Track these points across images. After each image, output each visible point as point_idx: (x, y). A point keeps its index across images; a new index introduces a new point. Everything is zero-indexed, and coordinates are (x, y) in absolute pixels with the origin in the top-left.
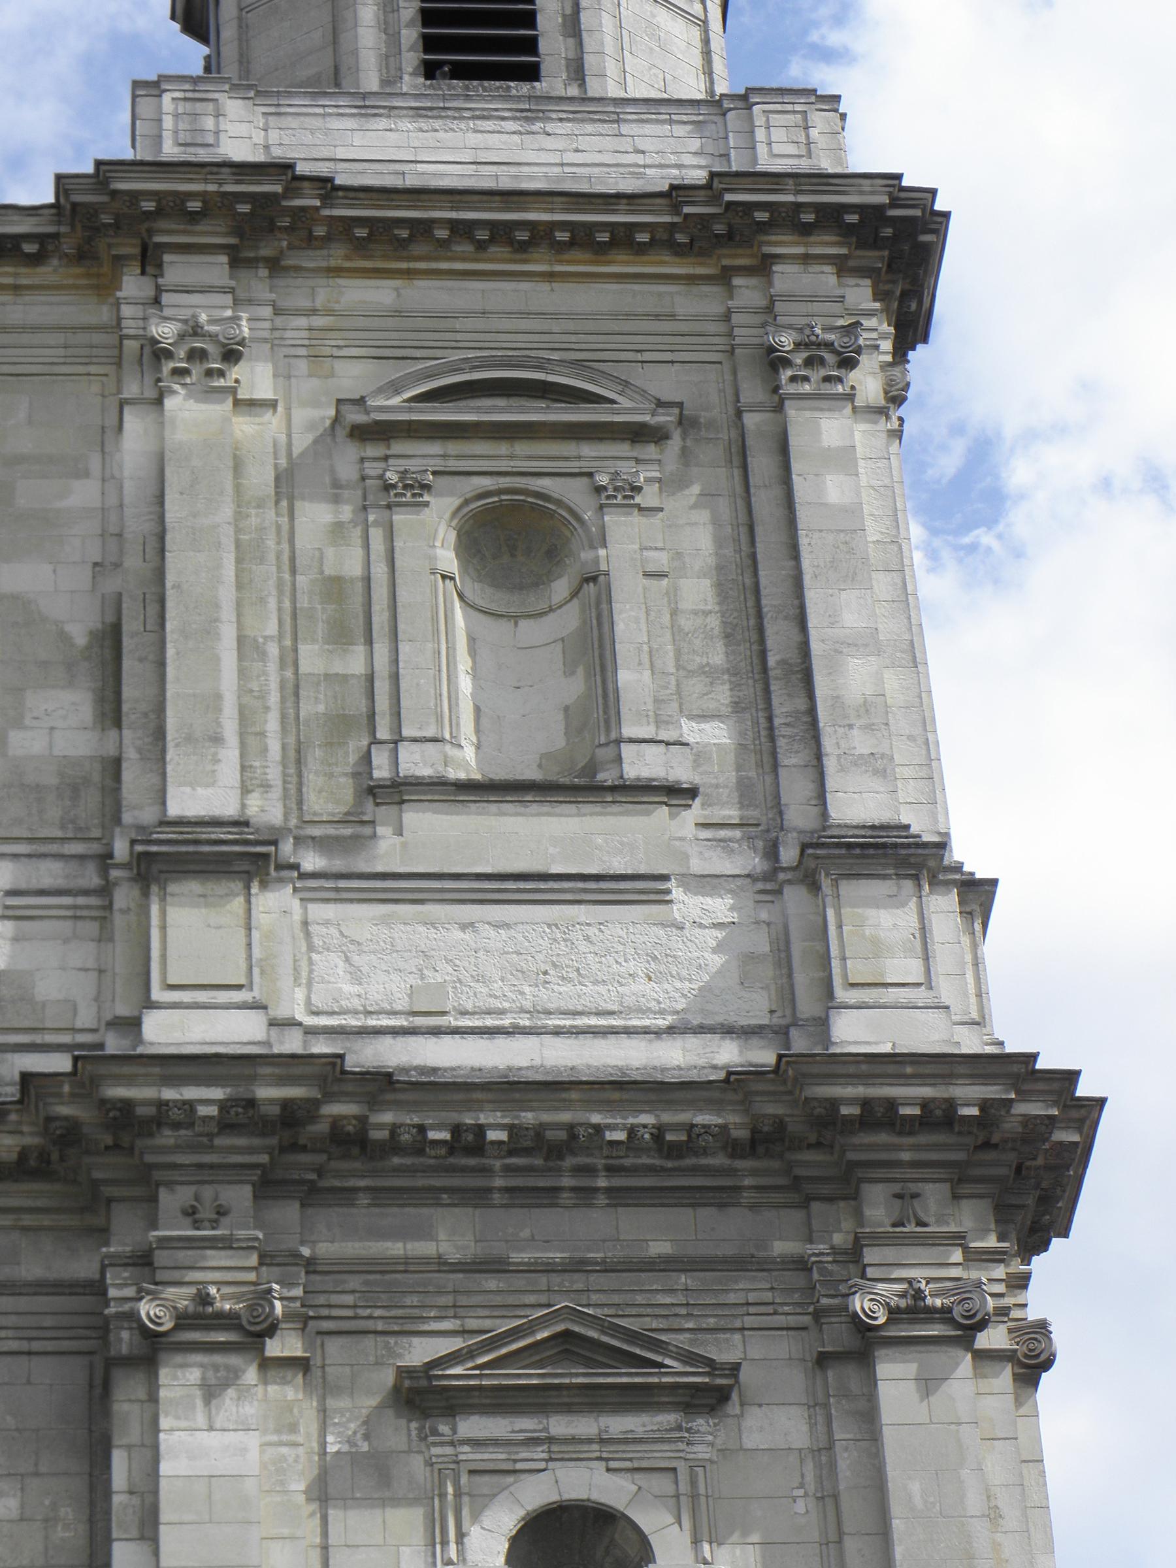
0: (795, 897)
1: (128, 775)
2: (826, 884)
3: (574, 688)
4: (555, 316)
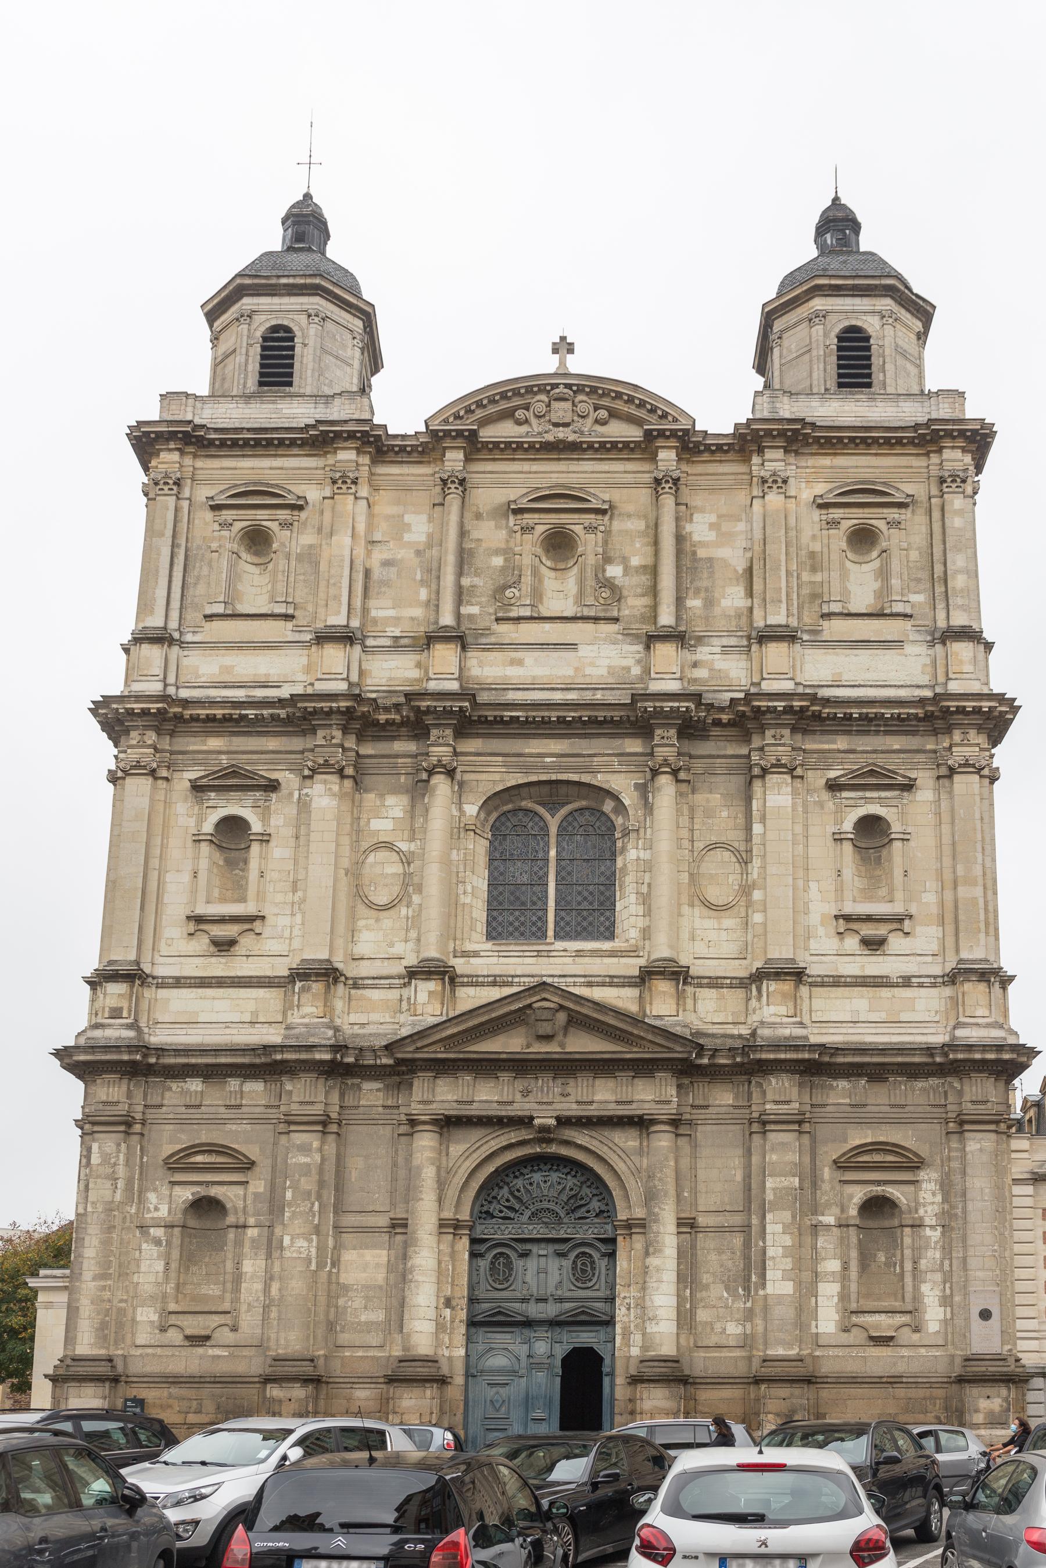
0: (939, 647)
1: (755, 612)
2: (948, 643)
3: (877, 585)
4: (877, 467)
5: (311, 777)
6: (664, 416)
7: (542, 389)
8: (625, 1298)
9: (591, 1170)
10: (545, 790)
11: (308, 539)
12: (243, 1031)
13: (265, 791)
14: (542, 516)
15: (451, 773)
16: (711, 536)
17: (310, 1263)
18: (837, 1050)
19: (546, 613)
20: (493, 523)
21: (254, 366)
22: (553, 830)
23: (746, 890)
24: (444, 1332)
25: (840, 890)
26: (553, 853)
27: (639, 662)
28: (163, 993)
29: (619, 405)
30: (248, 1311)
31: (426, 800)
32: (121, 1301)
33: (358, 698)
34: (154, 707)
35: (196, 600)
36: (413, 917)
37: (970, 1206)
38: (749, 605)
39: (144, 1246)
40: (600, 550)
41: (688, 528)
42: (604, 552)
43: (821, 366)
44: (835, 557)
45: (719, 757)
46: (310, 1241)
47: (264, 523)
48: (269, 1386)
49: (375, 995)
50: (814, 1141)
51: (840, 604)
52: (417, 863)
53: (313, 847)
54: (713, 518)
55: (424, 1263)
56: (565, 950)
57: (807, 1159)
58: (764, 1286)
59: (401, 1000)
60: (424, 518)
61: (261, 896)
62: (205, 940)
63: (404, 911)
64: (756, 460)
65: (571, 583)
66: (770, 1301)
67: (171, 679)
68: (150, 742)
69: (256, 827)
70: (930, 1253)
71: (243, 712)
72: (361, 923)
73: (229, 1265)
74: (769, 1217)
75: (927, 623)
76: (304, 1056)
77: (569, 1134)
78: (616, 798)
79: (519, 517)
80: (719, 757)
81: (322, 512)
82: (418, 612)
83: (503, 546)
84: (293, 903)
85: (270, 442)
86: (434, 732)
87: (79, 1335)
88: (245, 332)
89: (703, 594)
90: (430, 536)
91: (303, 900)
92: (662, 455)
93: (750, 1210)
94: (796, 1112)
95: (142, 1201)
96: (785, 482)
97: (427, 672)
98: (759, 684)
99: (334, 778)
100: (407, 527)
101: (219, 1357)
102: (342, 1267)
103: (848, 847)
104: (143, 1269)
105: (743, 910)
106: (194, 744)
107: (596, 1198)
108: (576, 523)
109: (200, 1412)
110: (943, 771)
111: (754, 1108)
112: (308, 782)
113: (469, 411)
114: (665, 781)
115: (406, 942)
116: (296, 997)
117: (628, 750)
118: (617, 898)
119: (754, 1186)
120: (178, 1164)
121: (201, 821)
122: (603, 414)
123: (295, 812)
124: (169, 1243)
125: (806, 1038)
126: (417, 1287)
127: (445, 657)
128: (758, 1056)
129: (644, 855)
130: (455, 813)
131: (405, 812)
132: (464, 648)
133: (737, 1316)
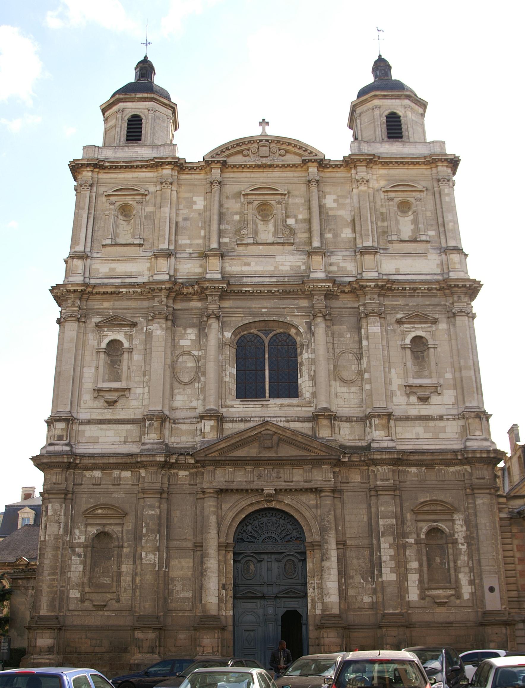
0: (443, 256)
3: (412, 227)
5: (152, 320)
6: (311, 153)
7: (255, 141)
8: (312, 583)
9: (292, 516)
10: (263, 324)
11: (150, 209)
12: (120, 446)
13: (130, 327)
14: (257, 197)
15: (218, 318)
16: (335, 205)
17: (156, 566)
18: (411, 453)
19: (260, 242)
20: (234, 200)
21: (124, 132)
22: (267, 344)
23: (360, 373)
24: (222, 602)
25: (406, 373)
26: (267, 356)
27: (304, 263)
28: (82, 427)
29: (290, 148)
30: (125, 592)
31: (206, 330)
32: (62, 587)
33: (175, 283)
34: (79, 289)
35: (98, 238)
36: (201, 388)
37: (480, 532)
38: (354, 236)
39: (73, 557)
40: (284, 212)
41: (324, 201)
42: (286, 213)
43: (380, 129)
44: (392, 215)
45: (344, 308)
46: (155, 555)
47: (130, 202)
48: (136, 632)
49: (183, 427)
50: (401, 500)
51: (396, 236)
52: (203, 361)
53: (153, 354)
54: (335, 197)
55: (212, 566)
56: (275, 404)
57: (399, 509)
58: (381, 576)
59: (196, 430)
60: (202, 198)
61: (128, 378)
62: (102, 401)
63: (196, 385)
64: (353, 171)
65: (271, 227)
66: (385, 584)
67: (87, 275)
68: (77, 305)
69: (126, 345)
70: (462, 557)
71: (121, 290)
72: (176, 391)
73: (115, 568)
74: (382, 540)
75: (437, 245)
76: (151, 459)
77: (280, 497)
78: (296, 328)
79: (246, 197)
80: (344, 308)
81: (156, 197)
82: (200, 241)
83: (239, 211)
84: (144, 382)
85: (132, 167)
86: (210, 298)
87: (42, 605)
88: (120, 118)
89: (332, 232)
90: (205, 206)
91: (149, 380)
92: (310, 170)
93: (372, 536)
94: (392, 485)
95: (72, 533)
96: (367, 181)
97: (205, 270)
98: (361, 274)
99: (163, 321)
100: (195, 203)
101: (110, 616)
102: (171, 568)
103: (408, 352)
104: (73, 569)
105: (360, 382)
106: (97, 305)
107: (295, 531)
108: (272, 200)
109: (101, 646)
110: (451, 315)
111: (371, 483)
112: (151, 322)
113: (222, 152)
114: (319, 320)
115: (198, 400)
116: (147, 429)
117: (301, 305)
118: (299, 377)
119: (373, 524)
120: (89, 513)
121: (100, 341)
122: (283, 152)
123: (144, 337)
124: (85, 556)
125: (395, 447)
126: (209, 579)
127: (214, 263)
128: (372, 457)
129: (312, 356)
130: (221, 337)
131: (196, 336)
132: (222, 257)
133: (368, 592)
